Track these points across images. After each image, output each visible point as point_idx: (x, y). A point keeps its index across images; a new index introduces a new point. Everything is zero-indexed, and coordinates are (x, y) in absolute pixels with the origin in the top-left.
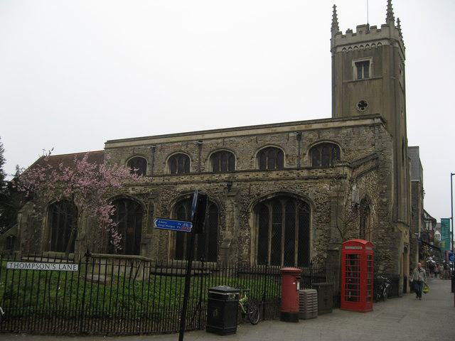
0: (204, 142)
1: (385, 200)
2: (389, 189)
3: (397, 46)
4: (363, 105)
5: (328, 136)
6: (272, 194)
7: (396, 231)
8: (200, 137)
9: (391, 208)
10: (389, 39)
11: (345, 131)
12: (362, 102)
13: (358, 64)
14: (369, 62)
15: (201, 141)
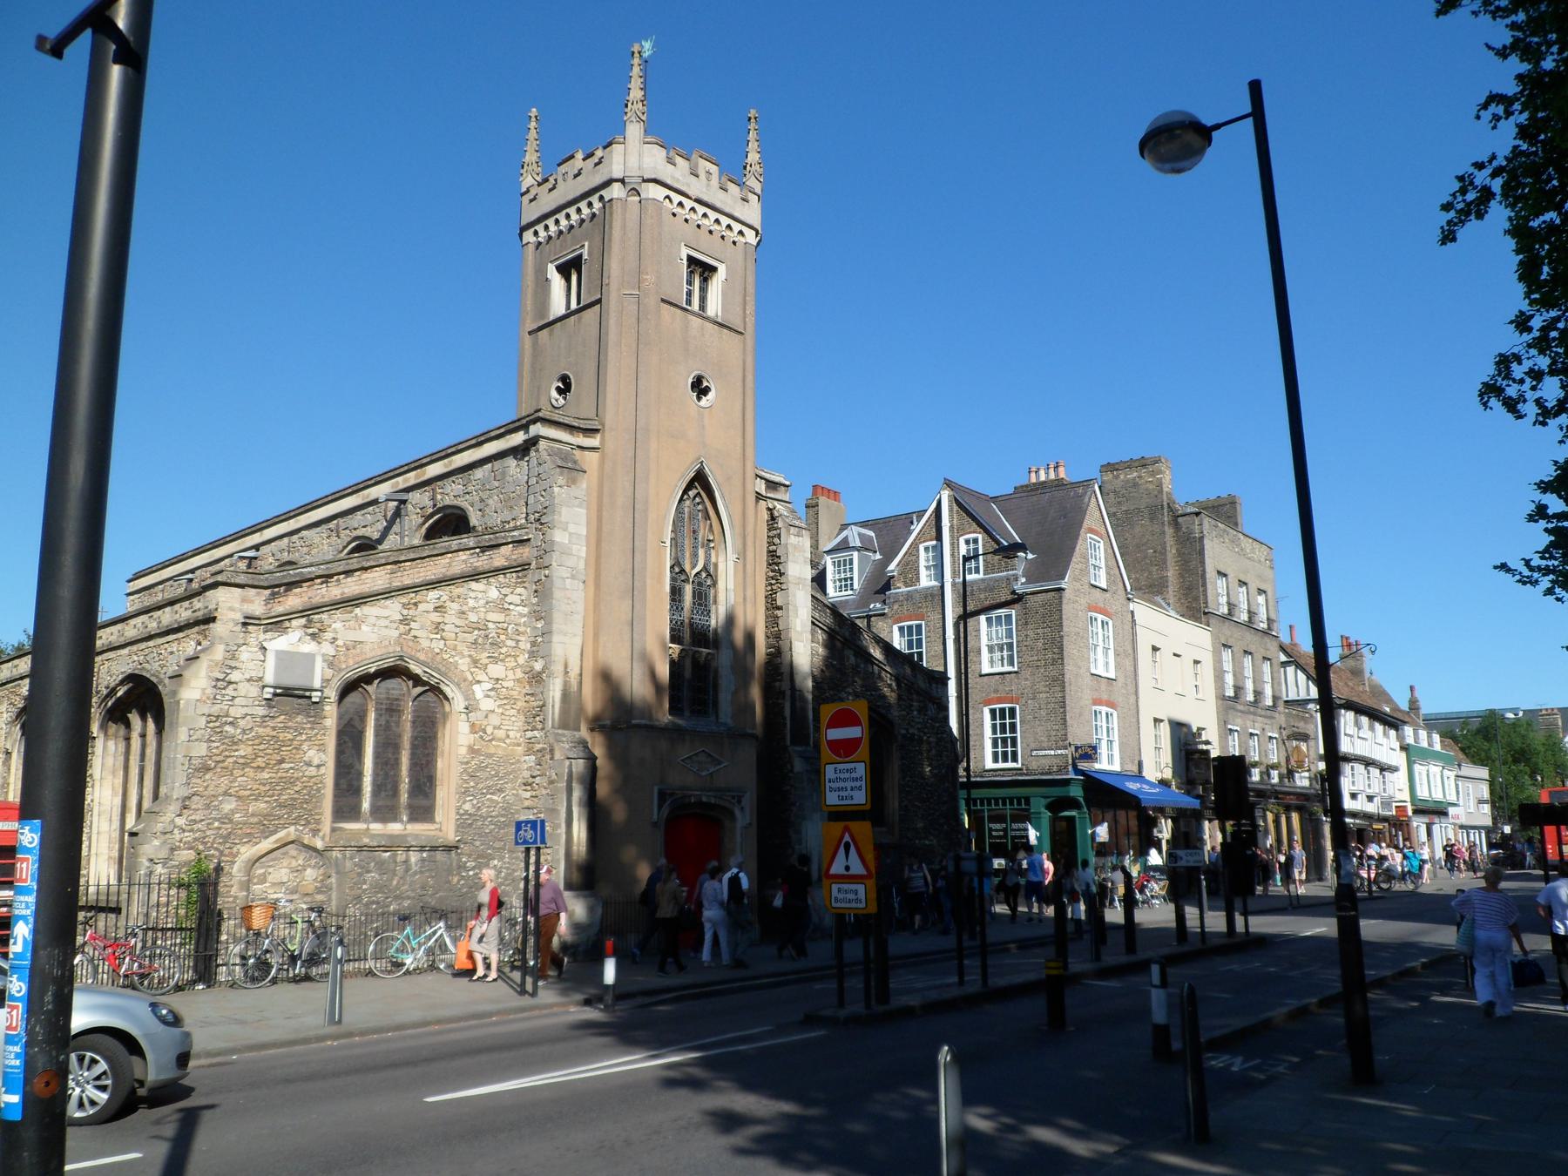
0: (264, 549)
1: (538, 666)
2: (547, 633)
3: (656, 192)
4: (565, 388)
5: (451, 493)
6: (122, 683)
7: (558, 756)
8: (256, 539)
9: (555, 692)
10: (622, 181)
11: (479, 473)
12: (565, 379)
13: (565, 270)
14: (580, 256)
15: (257, 547)
